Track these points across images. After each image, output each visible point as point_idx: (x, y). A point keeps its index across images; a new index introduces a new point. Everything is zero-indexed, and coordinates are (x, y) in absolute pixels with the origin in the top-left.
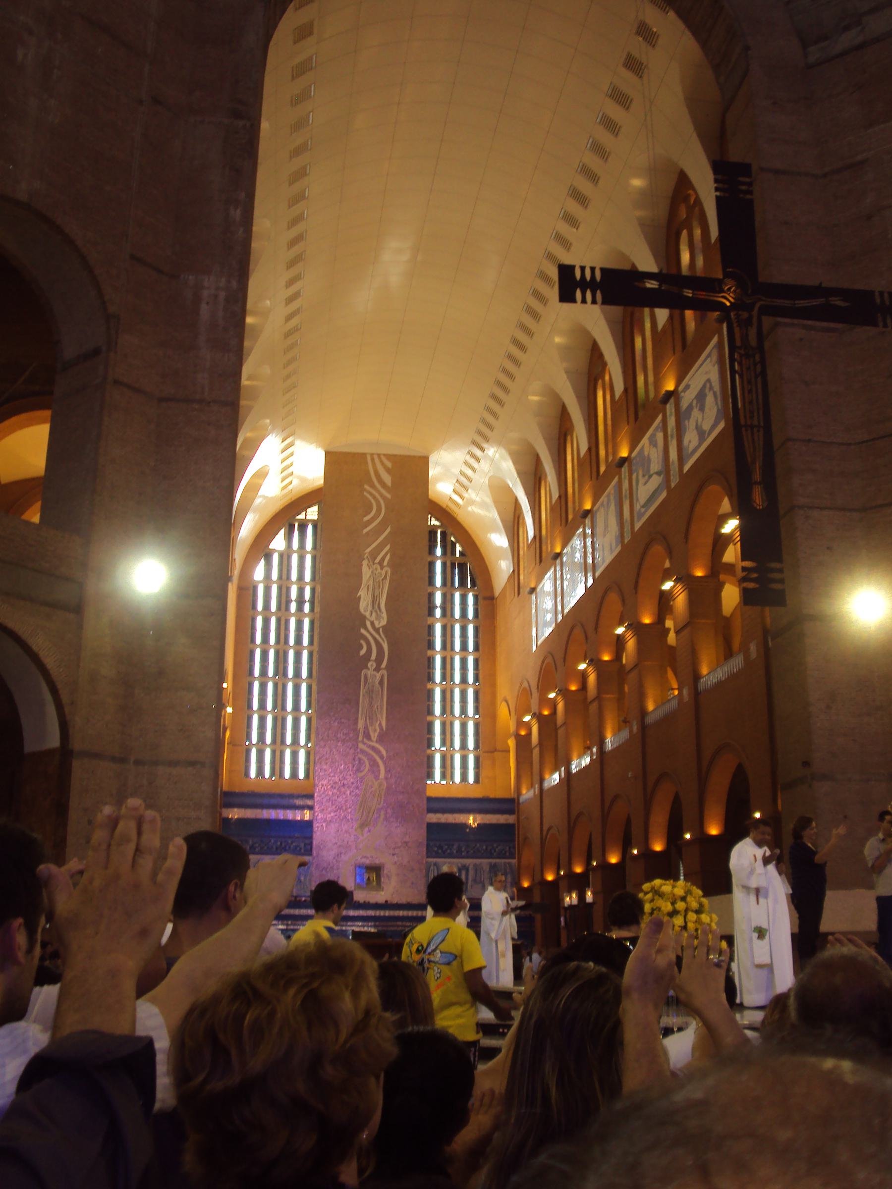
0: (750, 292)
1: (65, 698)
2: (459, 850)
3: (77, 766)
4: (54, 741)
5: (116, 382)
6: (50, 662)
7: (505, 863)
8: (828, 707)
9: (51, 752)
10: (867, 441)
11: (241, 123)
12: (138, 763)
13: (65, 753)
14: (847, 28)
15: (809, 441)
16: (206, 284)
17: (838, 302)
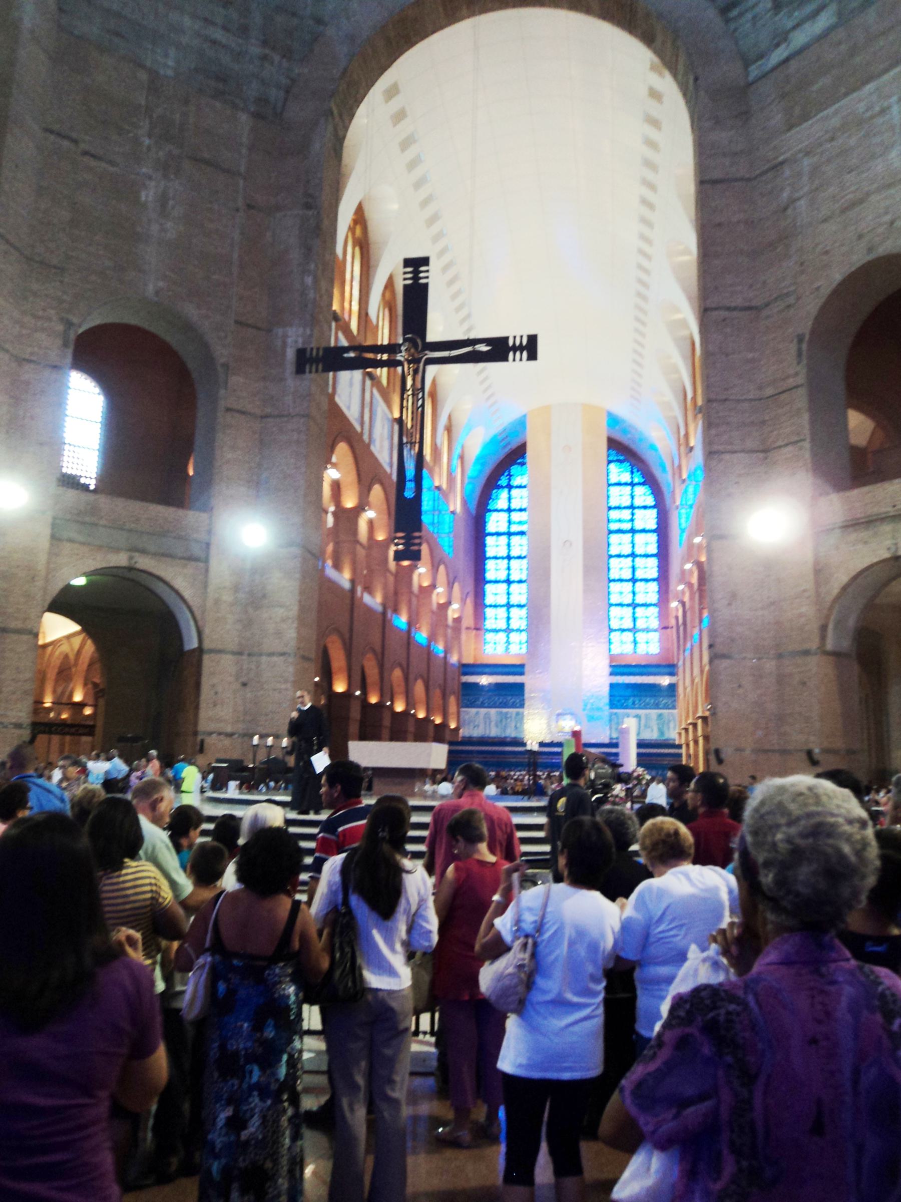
0: (420, 349)
1: (199, 617)
2: (634, 703)
3: (207, 660)
4: (194, 644)
5: (228, 410)
6: (187, 594)
7: (669, 713)
8: (730, 604)
9: (194, 650)
10: (773, 396)
11: (310, 213)
12: (249, 655)
13: (200, 650)
14: (777, 45)
15: (726, 400)
16: (290, 333)
17: (483, 348)
